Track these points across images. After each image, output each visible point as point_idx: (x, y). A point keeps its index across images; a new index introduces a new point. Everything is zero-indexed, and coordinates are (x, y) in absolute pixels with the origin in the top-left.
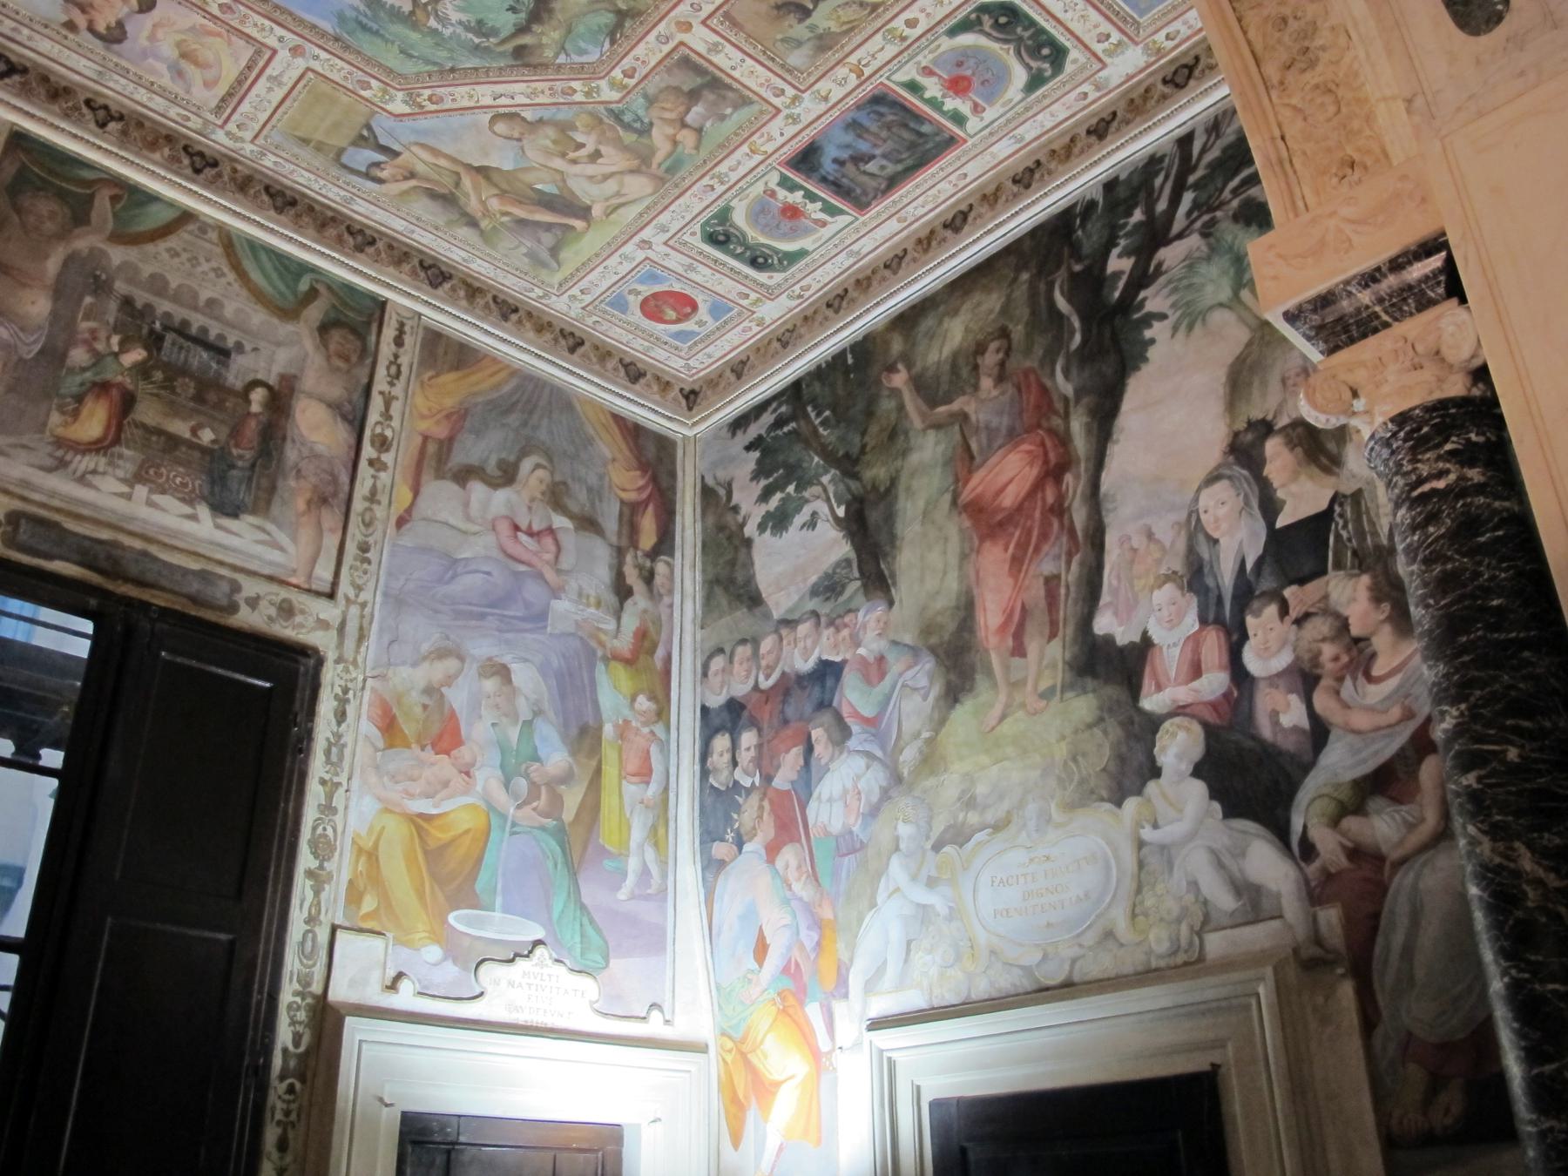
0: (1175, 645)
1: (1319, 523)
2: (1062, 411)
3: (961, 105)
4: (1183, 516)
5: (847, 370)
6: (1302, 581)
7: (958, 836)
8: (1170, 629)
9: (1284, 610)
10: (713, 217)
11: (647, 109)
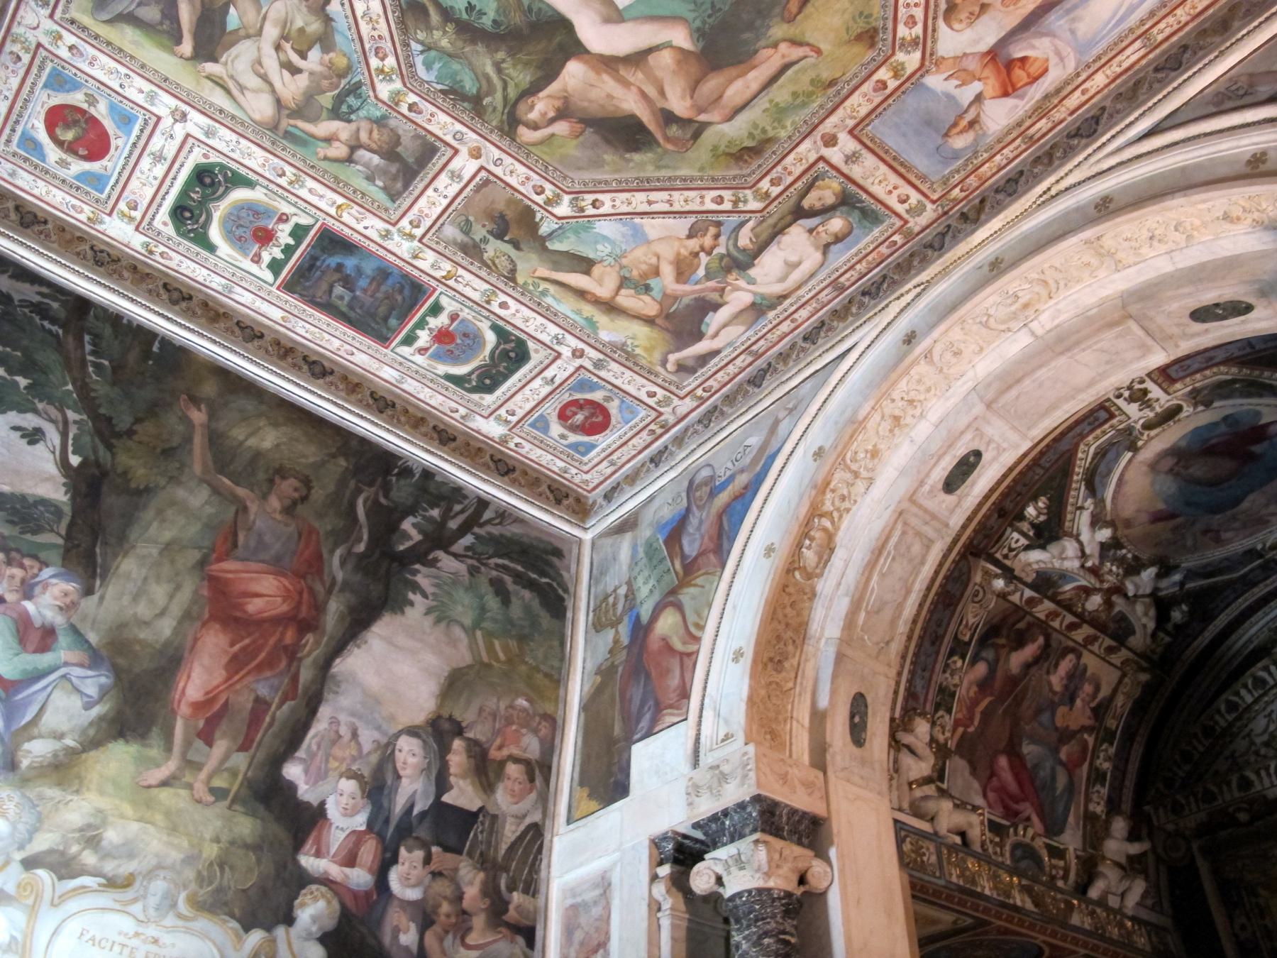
0: (342, 829)
1: (467, 819)
2: (327, 585)
3: (424, 337)
4: (384, 740)
5: (147, 354)
6: (447, 849)
7: (64, 866)
8: (345, 815)
9: (427, 860)
10: (231, 170)
11: (369, 119)
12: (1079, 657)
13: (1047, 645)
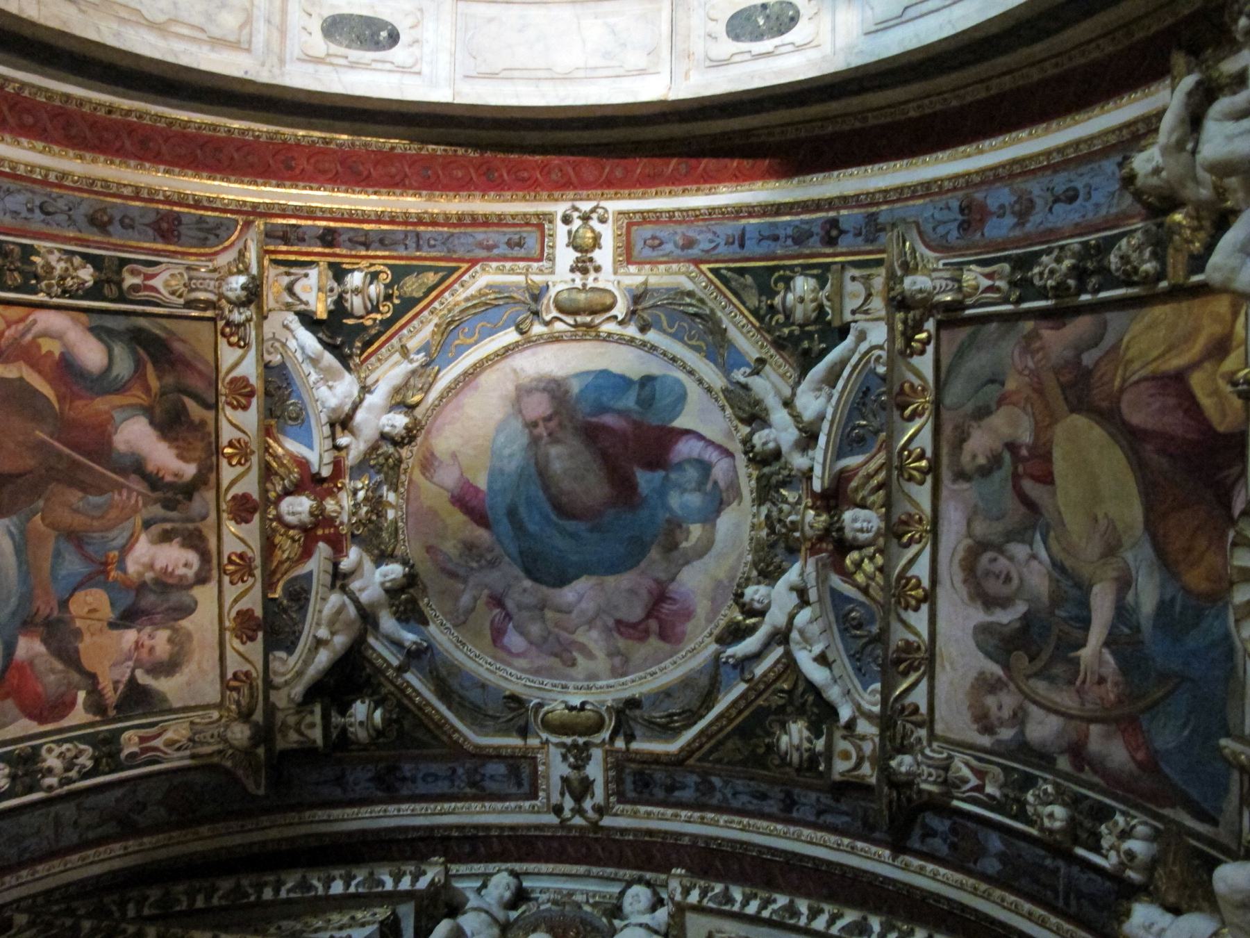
12: (201, 579)
13: (189, 490)
